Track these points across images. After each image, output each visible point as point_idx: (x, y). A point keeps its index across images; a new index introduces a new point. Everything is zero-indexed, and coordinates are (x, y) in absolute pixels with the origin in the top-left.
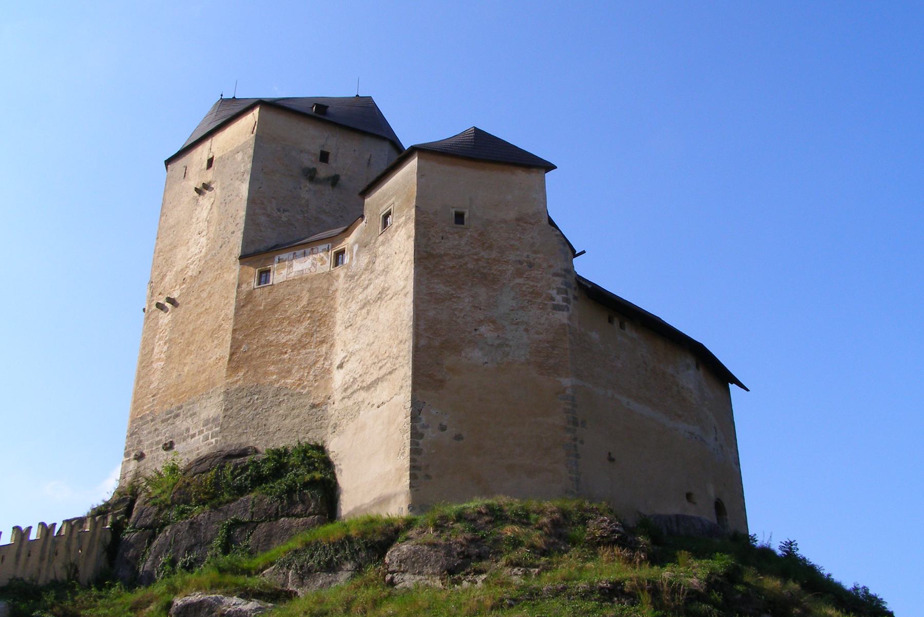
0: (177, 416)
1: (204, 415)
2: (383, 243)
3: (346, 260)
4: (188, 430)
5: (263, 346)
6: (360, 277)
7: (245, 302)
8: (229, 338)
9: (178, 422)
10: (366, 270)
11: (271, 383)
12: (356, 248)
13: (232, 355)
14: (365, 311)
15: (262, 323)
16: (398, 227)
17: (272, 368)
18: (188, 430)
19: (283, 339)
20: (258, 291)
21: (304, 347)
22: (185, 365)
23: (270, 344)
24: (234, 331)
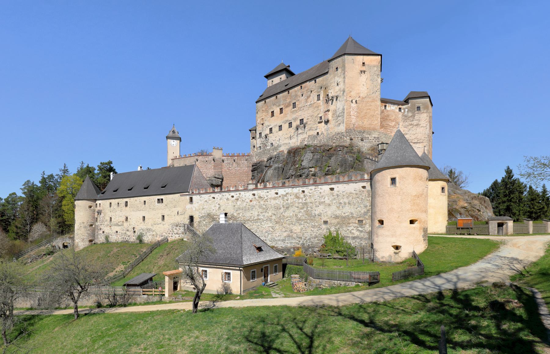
0: (364, 133)
1: (373, 136)
2: (418, 114)
3: (403, 111)
4: (368, 137)
5: (387, 124)
6: (409, 117)
7: (382, 112)
8: (379, 119)
9: (364, 135)
10: (411, 117)
11: (389, 134)
12: (406, 110)
13: (381, 124)
14: (411, 126)
15: (386, 119)
16: (423, 113)
17: (389, 130)
18: (368, 137)
19: (391, 124)
20: (385, 111)
21: (394, 128)
22: (364, 121)
23: (388, 125)
24: (381, 118)
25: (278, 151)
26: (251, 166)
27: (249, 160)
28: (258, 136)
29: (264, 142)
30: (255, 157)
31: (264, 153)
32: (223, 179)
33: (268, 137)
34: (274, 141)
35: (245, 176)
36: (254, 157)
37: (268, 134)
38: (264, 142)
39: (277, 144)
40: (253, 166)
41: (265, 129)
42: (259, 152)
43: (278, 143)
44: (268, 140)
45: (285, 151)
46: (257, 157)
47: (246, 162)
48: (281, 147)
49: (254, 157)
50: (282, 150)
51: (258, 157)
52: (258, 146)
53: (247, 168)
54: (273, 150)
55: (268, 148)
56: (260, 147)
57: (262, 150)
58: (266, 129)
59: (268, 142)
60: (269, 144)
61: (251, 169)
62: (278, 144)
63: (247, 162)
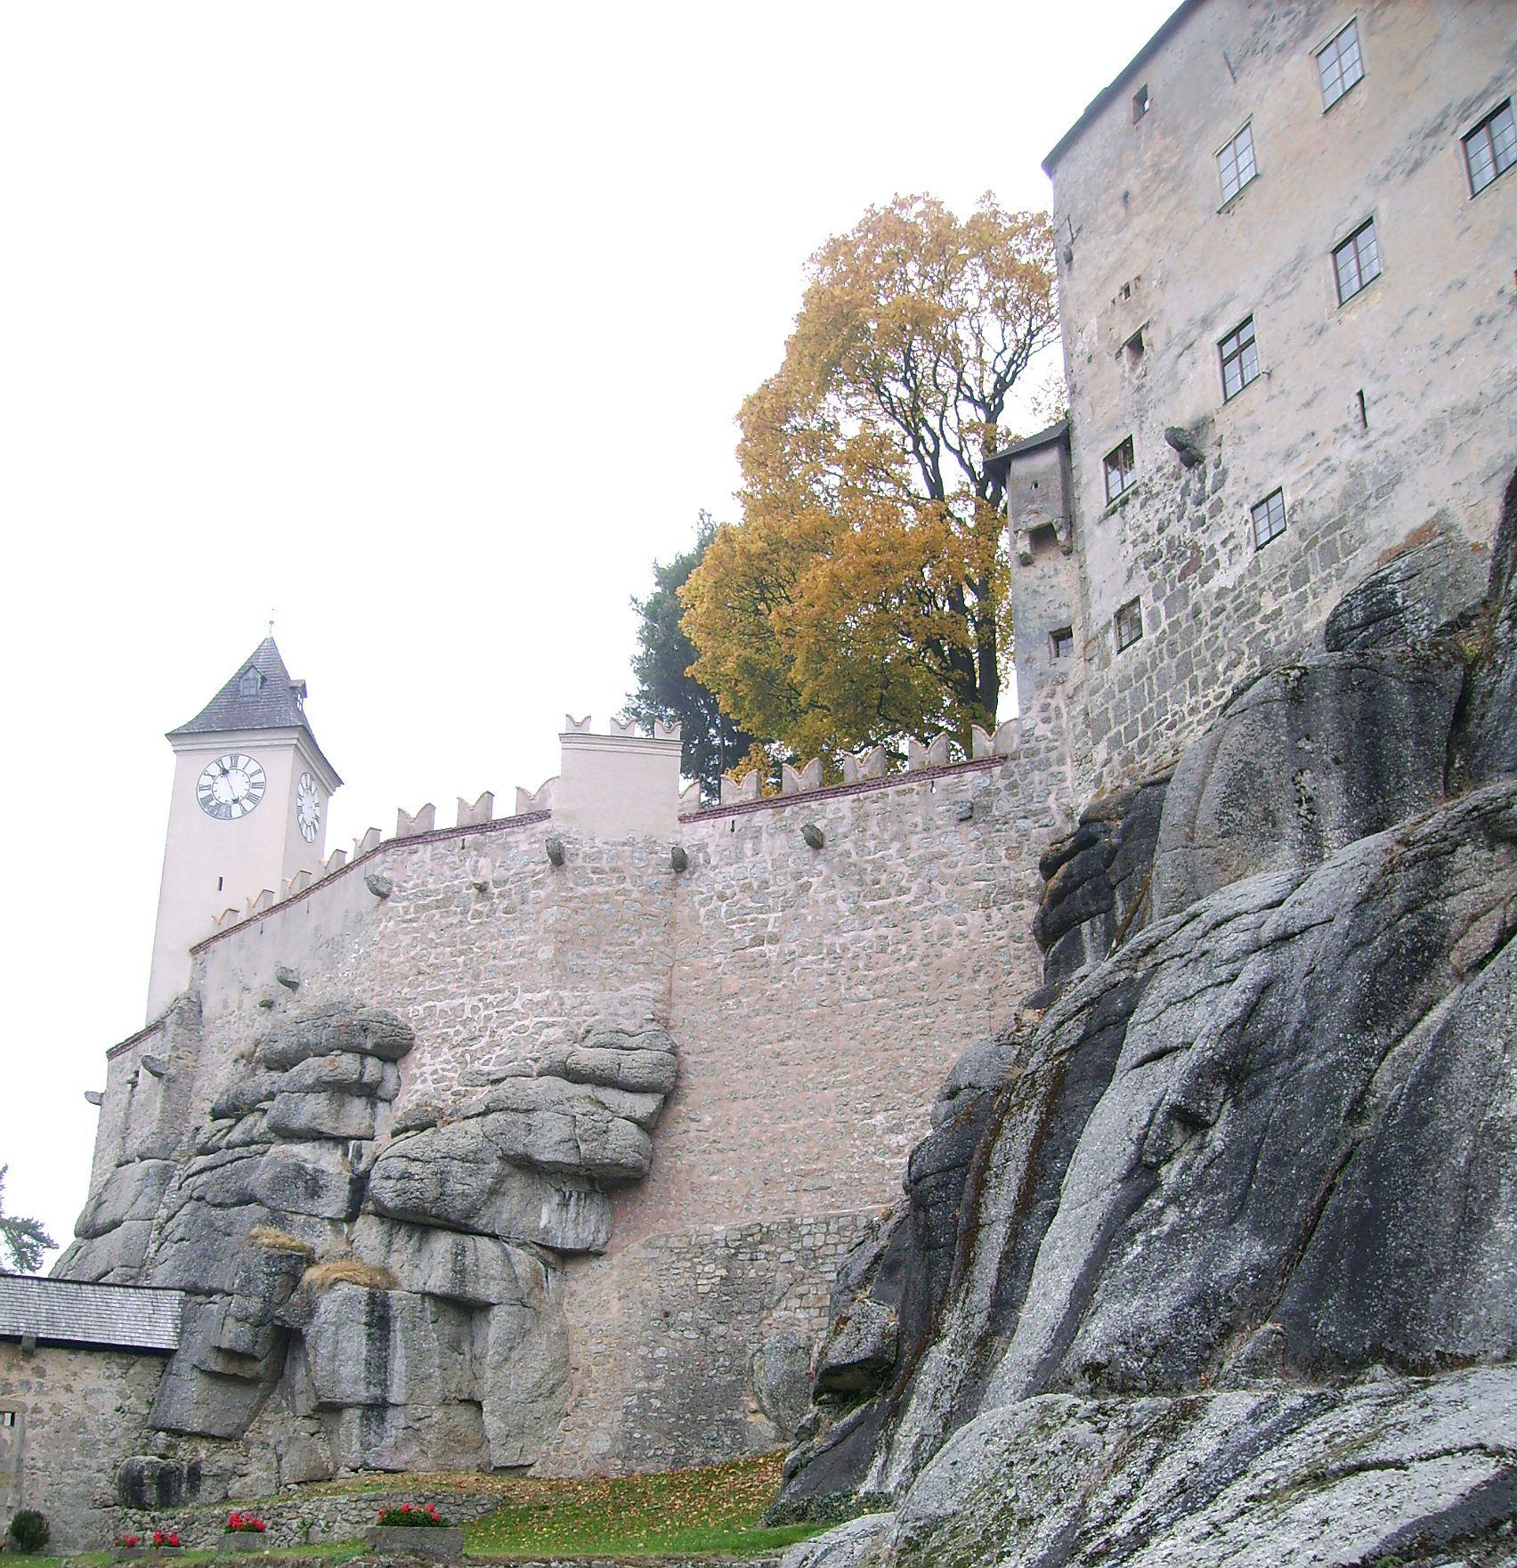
25: (1361, 565)
26: (1032, 878)
27: (1002, 805)
28: (1091, 502)
29: (1174, 529)
30: (1083, 759)
31: (1185, 667)
32: (669, 1094)
33: (1210, 454)
34: (1289, 455)
35: (954, 1015)
36: (1069, 770)
37: (1202, 425)
38: (1174, 529)
39: (1335, 484)
40: (1048, 868)
41: (1172, 375)
42: (1125, 683)
43: (1348, 451)
44: (1219, 483)
45: (1462, 520)
46: (1100, 752)
47: (960, 844)
48: (1401, 496)
49: (1069, 770)
50: (1419, 519)
51: (1115, 743)
52: (1104, 608)
53: (975, 918)
54: (1300, 578)
55: (1221, 579)
56: (1126, 615)
57: (1149, 636)
58: (1183, 363)
59: (1217, 507)
60: (1236, 521)
61: (1031, 911)
62: (1355, 474)
63: (982, 844)
